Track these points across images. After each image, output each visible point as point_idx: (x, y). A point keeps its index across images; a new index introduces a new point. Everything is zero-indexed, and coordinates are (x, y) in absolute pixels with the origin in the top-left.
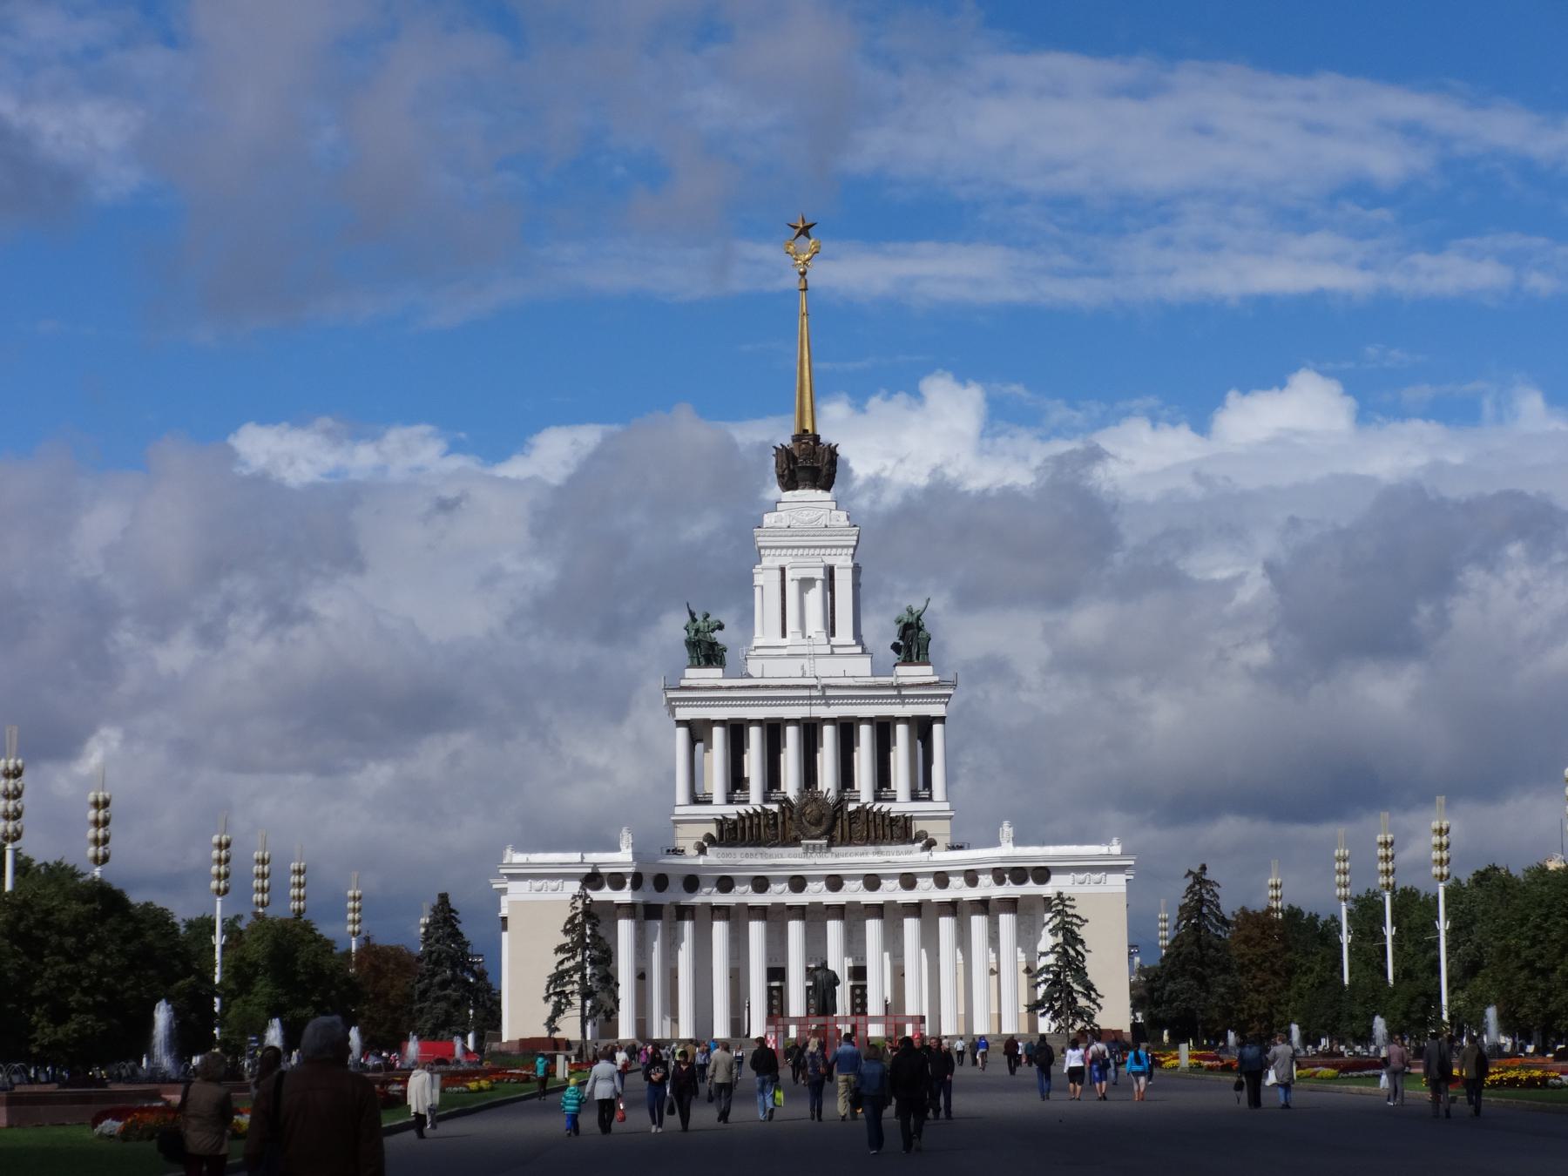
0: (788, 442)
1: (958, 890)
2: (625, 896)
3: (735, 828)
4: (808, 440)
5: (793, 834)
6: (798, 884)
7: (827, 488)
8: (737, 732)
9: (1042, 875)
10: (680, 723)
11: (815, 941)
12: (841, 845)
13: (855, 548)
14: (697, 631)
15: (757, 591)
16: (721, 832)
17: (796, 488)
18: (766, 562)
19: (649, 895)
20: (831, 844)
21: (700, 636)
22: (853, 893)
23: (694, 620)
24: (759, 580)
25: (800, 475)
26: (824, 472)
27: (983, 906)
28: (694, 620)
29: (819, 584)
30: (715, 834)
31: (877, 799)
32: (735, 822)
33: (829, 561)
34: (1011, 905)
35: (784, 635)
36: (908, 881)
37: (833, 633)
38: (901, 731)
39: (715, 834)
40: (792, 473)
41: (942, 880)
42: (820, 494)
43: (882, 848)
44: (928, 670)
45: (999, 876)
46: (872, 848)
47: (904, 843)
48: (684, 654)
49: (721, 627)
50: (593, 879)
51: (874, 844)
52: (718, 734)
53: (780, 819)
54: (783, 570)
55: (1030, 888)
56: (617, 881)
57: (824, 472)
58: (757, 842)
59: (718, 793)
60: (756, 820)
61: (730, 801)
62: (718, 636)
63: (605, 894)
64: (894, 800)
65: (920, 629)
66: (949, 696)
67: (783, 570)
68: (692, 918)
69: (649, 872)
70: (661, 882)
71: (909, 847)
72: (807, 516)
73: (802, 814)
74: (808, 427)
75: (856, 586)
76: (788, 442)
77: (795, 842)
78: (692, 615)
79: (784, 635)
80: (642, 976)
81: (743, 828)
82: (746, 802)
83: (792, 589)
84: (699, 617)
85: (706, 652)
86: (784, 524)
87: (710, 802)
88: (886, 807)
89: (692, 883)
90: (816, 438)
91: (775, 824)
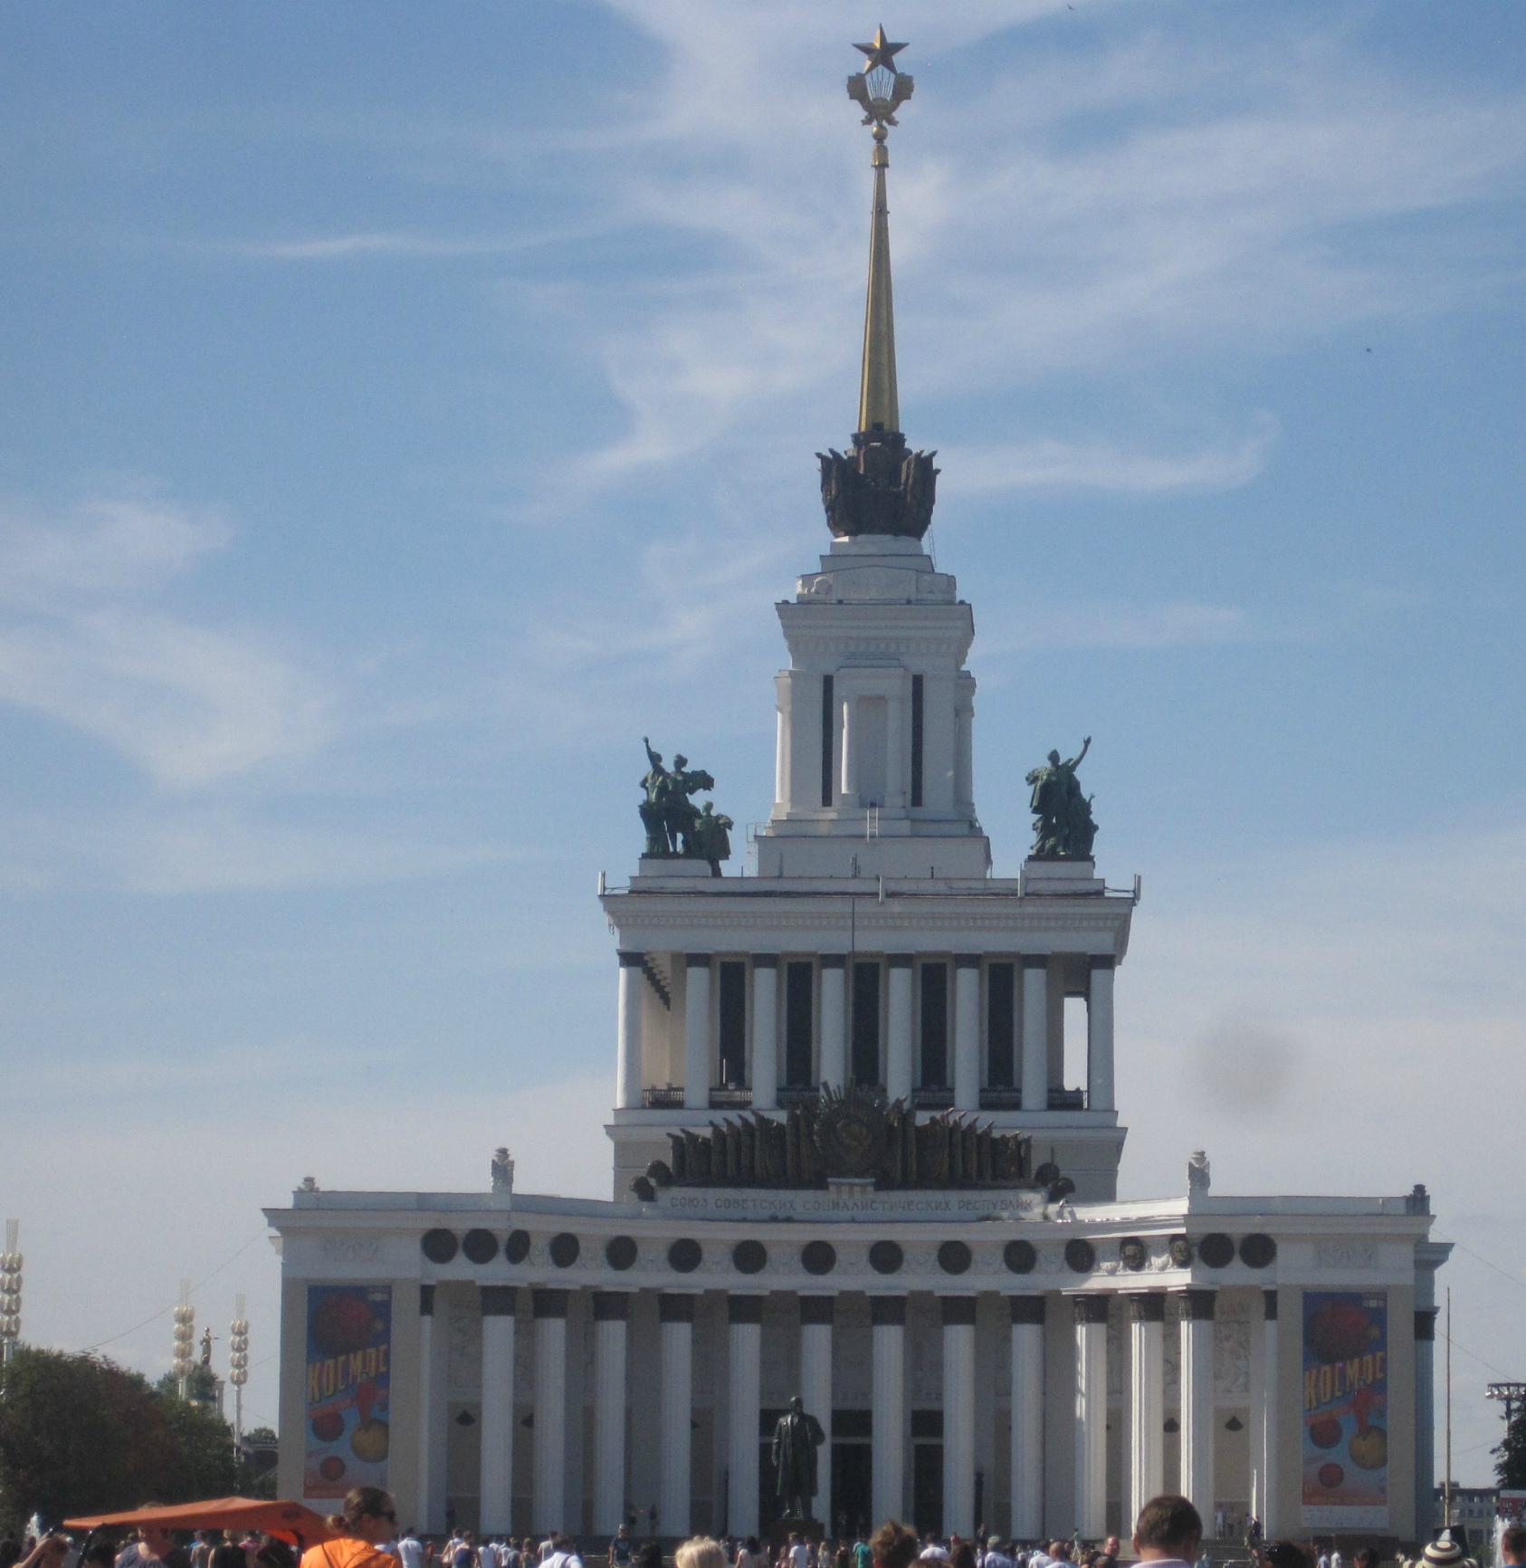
0: (845, 447)
1: (1109, 1279)
2: (498, 1272)
4: (881, 436)
8: (732, 979)
9: (1259, 1250)
10: (629, 959)
11: (782, 1364)
14: (662, 791)
19: (538, 1271)
20: (884, 1183)
23: (658, 770)
27: (1154, 1305)
28: (658, 770)
30: (669, 1161)
31: (985, 1105)
32: (706, 1141)
33: (918, 665)
34: (1200, 1303)
35: (827, 801)
36: (1020, 1256)
37: (917, 800)
38: (1033, 983)
39: (669, 1161)
41: (1081, 1255)
42: (903, 544)
45: (1185, 1250)
49: (705, 781)
50: (438, 1245)
51: (962, 1186)
52: (699, 984)
54: (828, 682)
55: (1237, 1274)
56: (480, 1245)
58: (746, 1178)
59: (696, 1094)
61: (714, 1105)
62: (698, 799)
63: (460, 1269)
64: (1016, 1106)
65: (1074, 787)
67: (828, 682)
68: (621, 1315)
69: (542, 1229)
70: (565, 1249)
76: (845, 447)
77: (820, 1184)
78: (655, 759)
79: (827, 801)
80: (525, 1421)
82: (744, 1105)
84: (668, 765)
86: (834, 598)
87: (679, 1105)
88: (985, 1119)
89: (622, 1252)
90: (900, 439)
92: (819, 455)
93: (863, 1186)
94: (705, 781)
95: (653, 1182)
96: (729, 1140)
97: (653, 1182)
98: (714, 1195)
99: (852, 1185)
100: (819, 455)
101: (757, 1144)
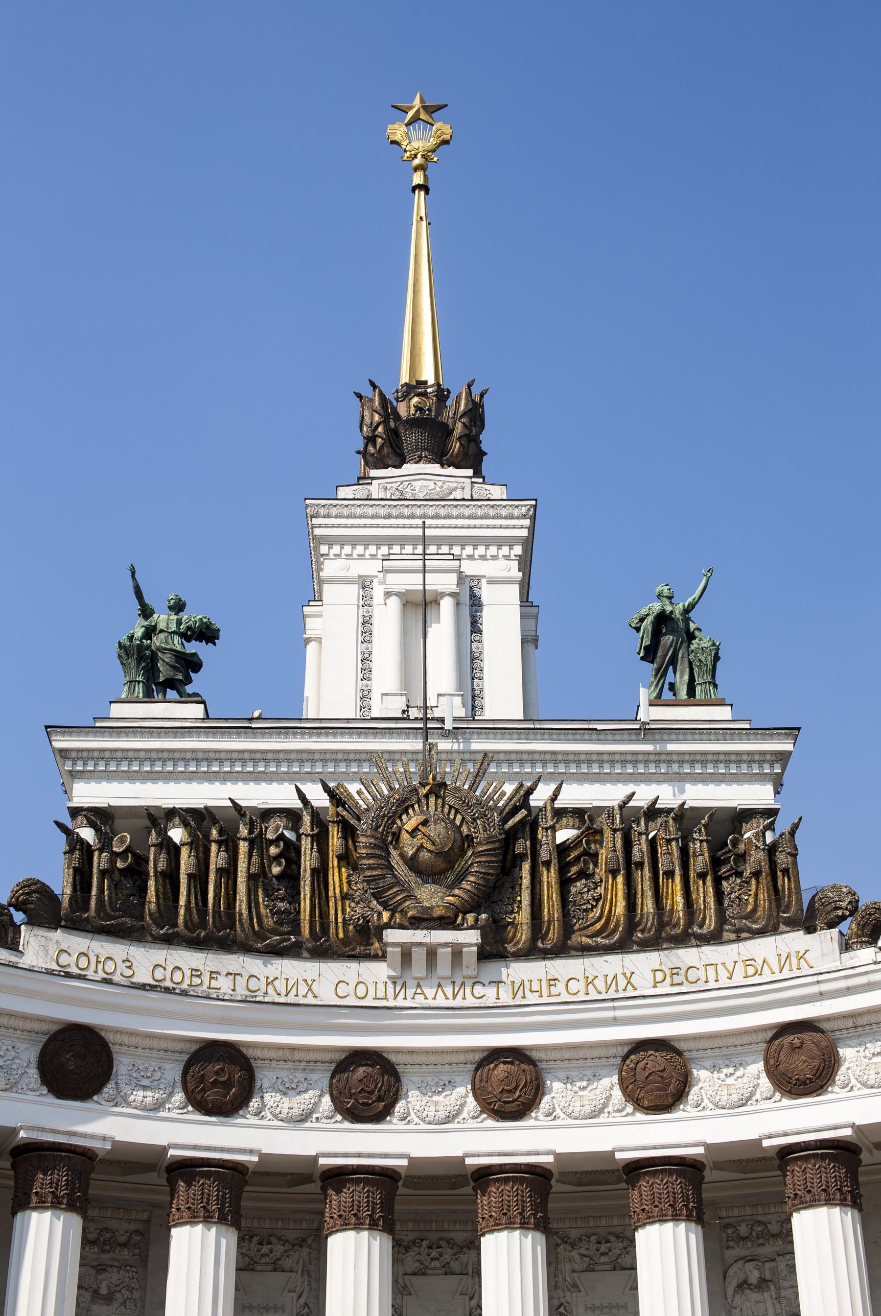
3: (137, 872)
5: (355, 910)
6: (367, 1085)
7: (472, 458)
12: (531, 952)
13: (528, 544)
14: (150, 631)
15: (311, 648)
16: (82, 877)
17: (399, 466)
18: (330, 569)
21: (158, 641)
22: (584, 1124)
24: (313, 627)
25: (410, 438)
26: (459, 429)
28: (146, 612)
29: (447, 604)
40: (394, 440)
43: (688, 956)
44: (723, 713)
46: (642, 965)
47: (770, 929)
48: (116, 675)
49: (207, 633)
53: (308, 860)
57: (459, 429)
58: (216, 933)
60: (217, 858)
62: (192, 647)
66: (783, 757)
71: (795, 940)
72: (421, 488)
73: (387, 838)
74: (428, 374)
75: (529, 641)
77: (362, 943)
81: (170, 877)
83: (388, 617)
85: (162, 667)
91: (291, 877)
92: (360, 397)
93: (457, 951)
94: (207, 633)
95: (18, 917)
96: (185, 852)
97: (18, 917)
98: (145, 961)
99: (432, 952)
100: (360, 397)
101: (242, 866)
